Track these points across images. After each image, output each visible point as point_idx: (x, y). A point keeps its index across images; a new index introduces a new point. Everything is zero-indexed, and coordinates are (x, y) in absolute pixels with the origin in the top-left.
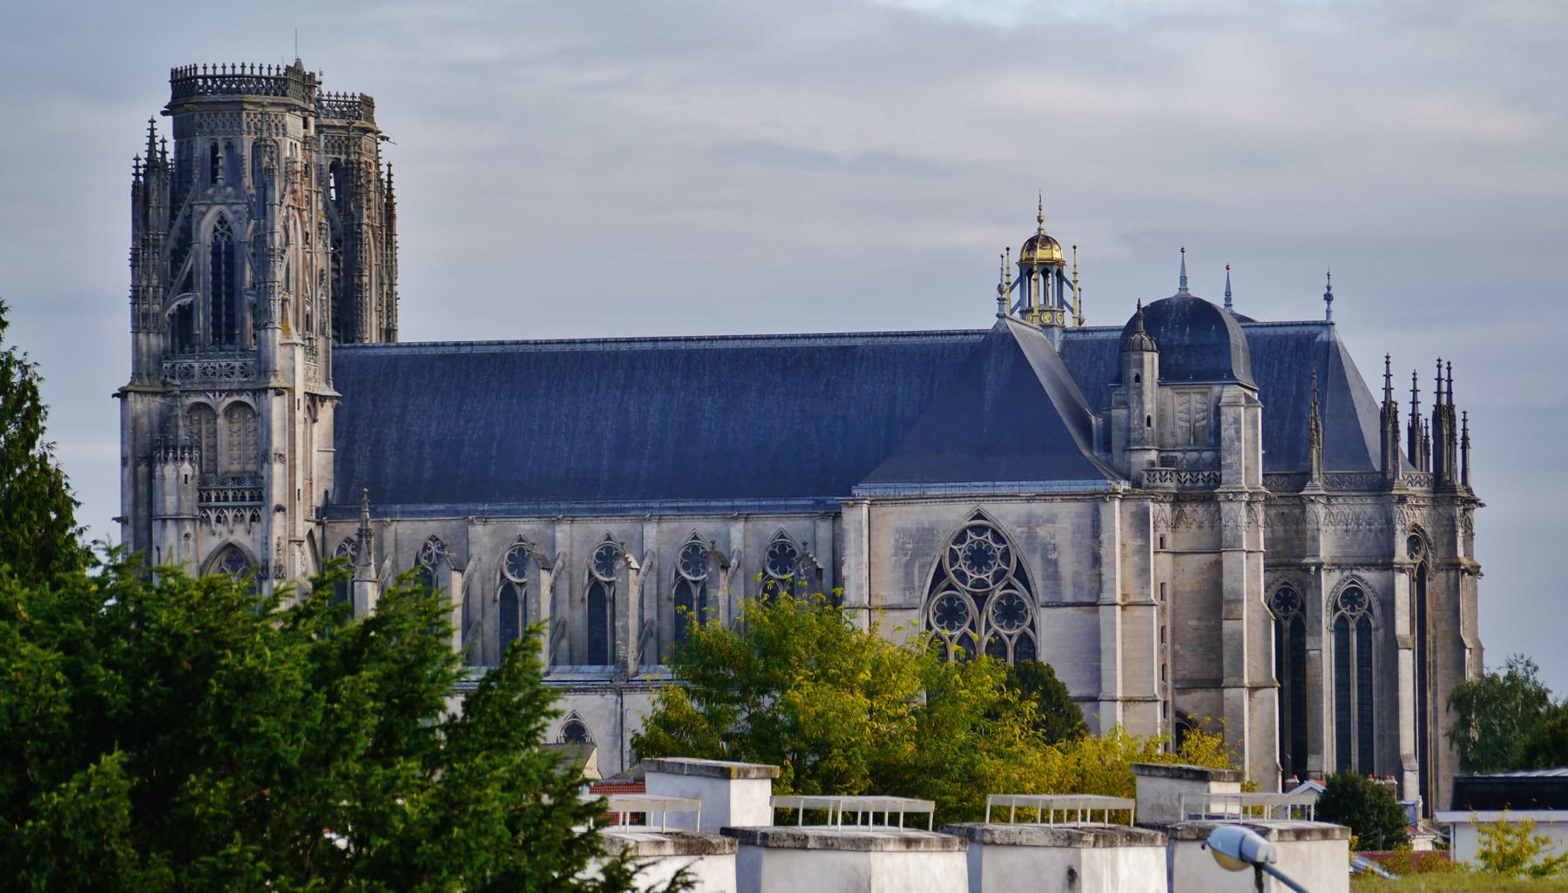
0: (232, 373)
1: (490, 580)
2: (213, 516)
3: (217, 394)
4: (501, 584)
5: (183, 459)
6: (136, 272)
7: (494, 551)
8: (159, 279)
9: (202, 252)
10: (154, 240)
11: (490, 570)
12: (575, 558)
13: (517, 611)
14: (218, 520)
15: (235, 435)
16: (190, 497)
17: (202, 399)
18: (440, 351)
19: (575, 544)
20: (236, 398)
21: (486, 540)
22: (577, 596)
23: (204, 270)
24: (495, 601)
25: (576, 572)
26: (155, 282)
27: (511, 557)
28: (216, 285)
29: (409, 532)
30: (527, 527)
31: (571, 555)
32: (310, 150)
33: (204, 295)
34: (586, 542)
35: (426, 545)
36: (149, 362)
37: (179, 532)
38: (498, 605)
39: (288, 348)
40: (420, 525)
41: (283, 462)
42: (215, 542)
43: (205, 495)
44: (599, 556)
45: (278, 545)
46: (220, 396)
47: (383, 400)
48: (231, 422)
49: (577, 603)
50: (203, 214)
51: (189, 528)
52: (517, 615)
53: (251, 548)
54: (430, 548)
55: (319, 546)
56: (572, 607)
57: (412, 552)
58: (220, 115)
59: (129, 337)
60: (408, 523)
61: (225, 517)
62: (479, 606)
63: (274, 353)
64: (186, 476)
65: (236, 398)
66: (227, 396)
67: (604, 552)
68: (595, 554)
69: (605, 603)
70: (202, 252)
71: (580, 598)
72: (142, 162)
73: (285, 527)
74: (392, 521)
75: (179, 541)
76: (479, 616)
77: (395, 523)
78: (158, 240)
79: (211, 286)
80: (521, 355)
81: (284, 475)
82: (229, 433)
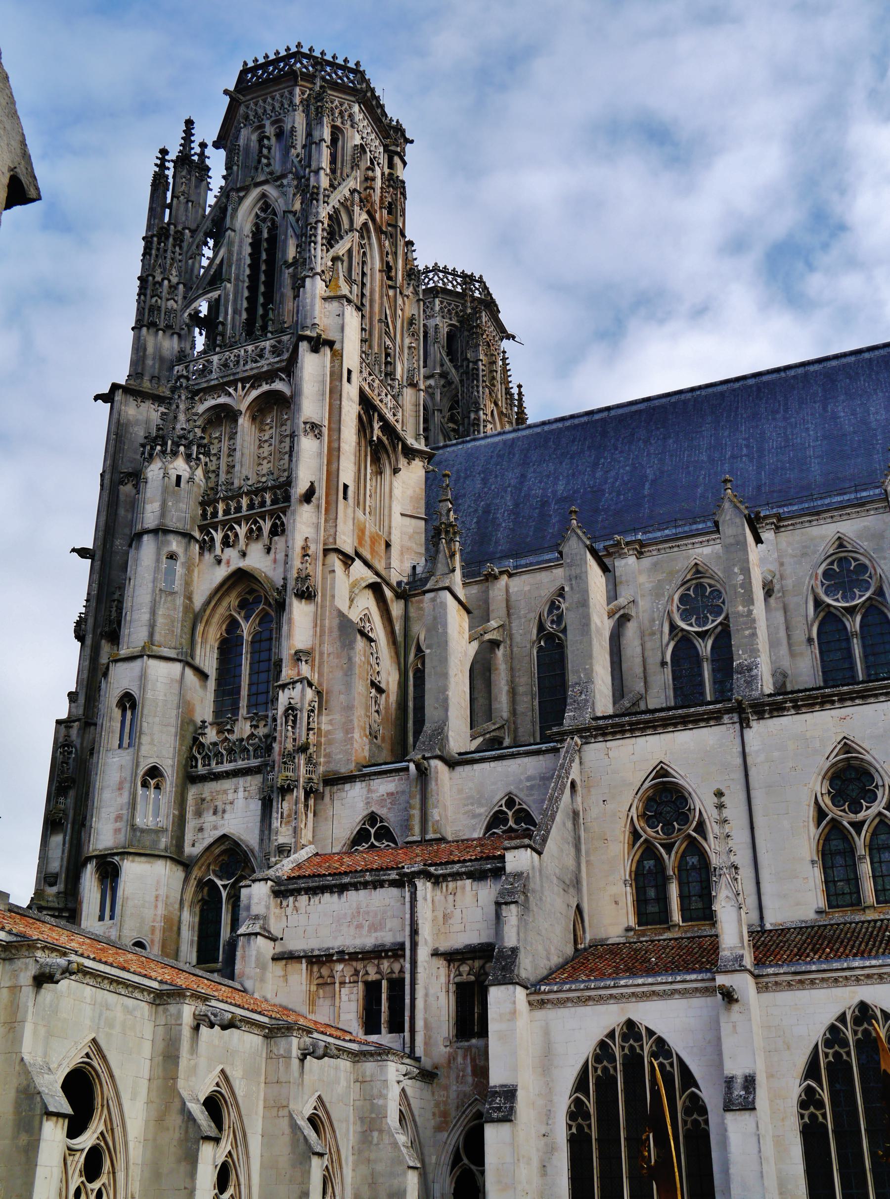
0: (261, 356)
1: (653, 634)
2: (218, 537)
3: (240, 385)
4: (671, 638)
5: (175, 454)
6: (146, 262)
7: (657, 592)
8: (179, 275)
9: (237, 240)
10: (176, 232)
11: (653, 620)
12: (789, 583)
13: (701, 675)
14: (226, 543)
15: (266, 445)
16: (183, 506)
17: (223, 400)
18: (568, 423)
19: (786, 560)
20: (265, 387)
21: (643, 579)
22: (800, 635)
23: (239, 260)
24: (663, 664)
25: (793, 601)
26: (174, 280)
27: (683, 599)
28: (253, 278)
29: (527, 588)
30: (707, 550)
31: (782, 577)
32: (395, 188)
33: (236, 287)
34: (804, 555)
35: (553, 603)
36: (154, 364)
37: (159, 550)
38: (668, 670)
39: (335, 304)
40: (544, 576)
41: (318, 436)
42: (221, 573)
43: (210, 510)
44: (827, 574)
45: (305, 548)
46: (243, 388)
47: (496, 477)
48: (262, 430)
49: (804, 648)
50: (241, 199)
51: (175, 544)
52: (702, 684)
53: (270, 574)
54: (559, 608)
55: (398, 627)
56: (792, 654)
57: (532, 615)
58: (269, 100)
59: (129, 337)
60: (525, 577)
61: (236, 535)
62: (639, 670)
63: (313, 305)
64: (179, 478)
65: (265, 387)
66: (253, 387)
67: (835, 567)
68: (820, 571)
69: (848, 640)
70: (237, 240)
71: (803, 638)
72: (172, 155)
73: (317, 527)
74: (501, 573)
75: (158, 560)
76: (640, 687)
77: (505, 577)
78: (182, 234)
79: (247, 280)
80: (674, 405)
81: (320, 454)
82: (257, 443)
